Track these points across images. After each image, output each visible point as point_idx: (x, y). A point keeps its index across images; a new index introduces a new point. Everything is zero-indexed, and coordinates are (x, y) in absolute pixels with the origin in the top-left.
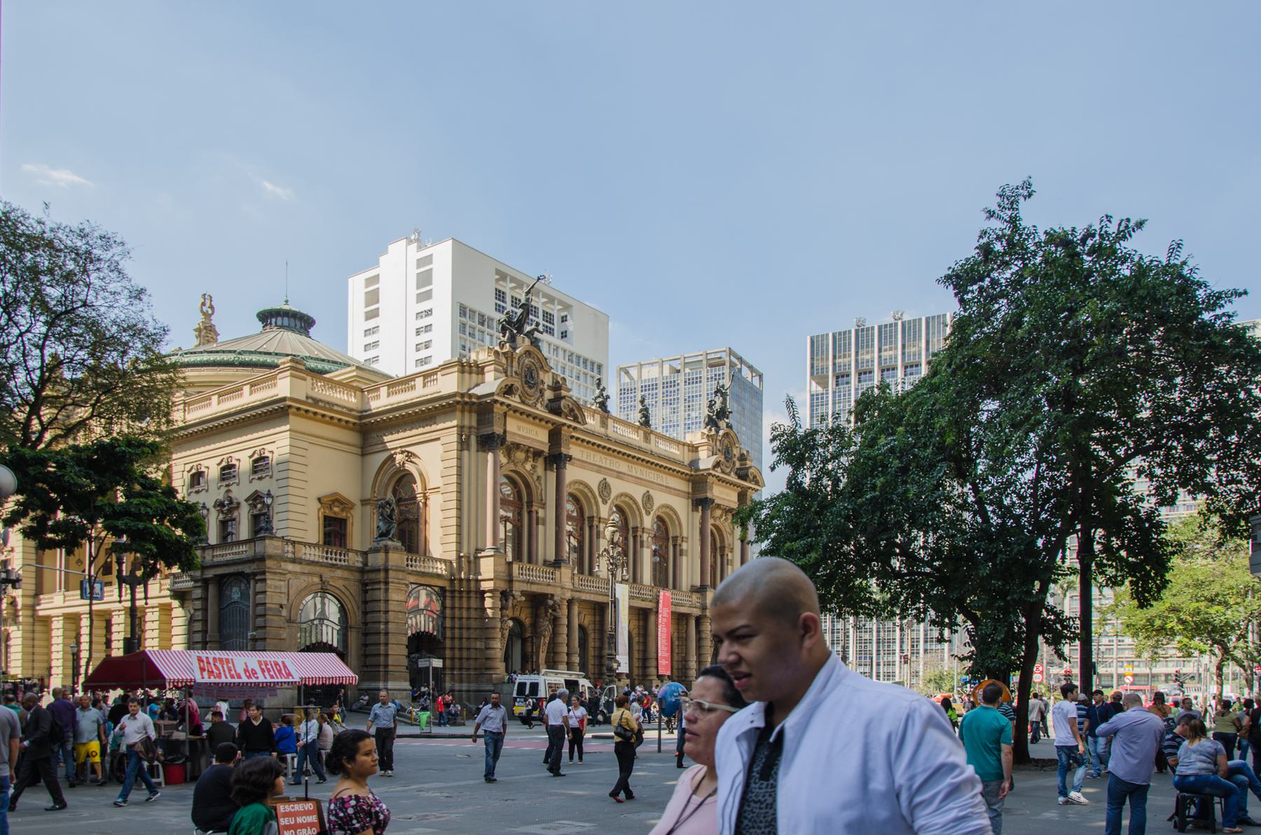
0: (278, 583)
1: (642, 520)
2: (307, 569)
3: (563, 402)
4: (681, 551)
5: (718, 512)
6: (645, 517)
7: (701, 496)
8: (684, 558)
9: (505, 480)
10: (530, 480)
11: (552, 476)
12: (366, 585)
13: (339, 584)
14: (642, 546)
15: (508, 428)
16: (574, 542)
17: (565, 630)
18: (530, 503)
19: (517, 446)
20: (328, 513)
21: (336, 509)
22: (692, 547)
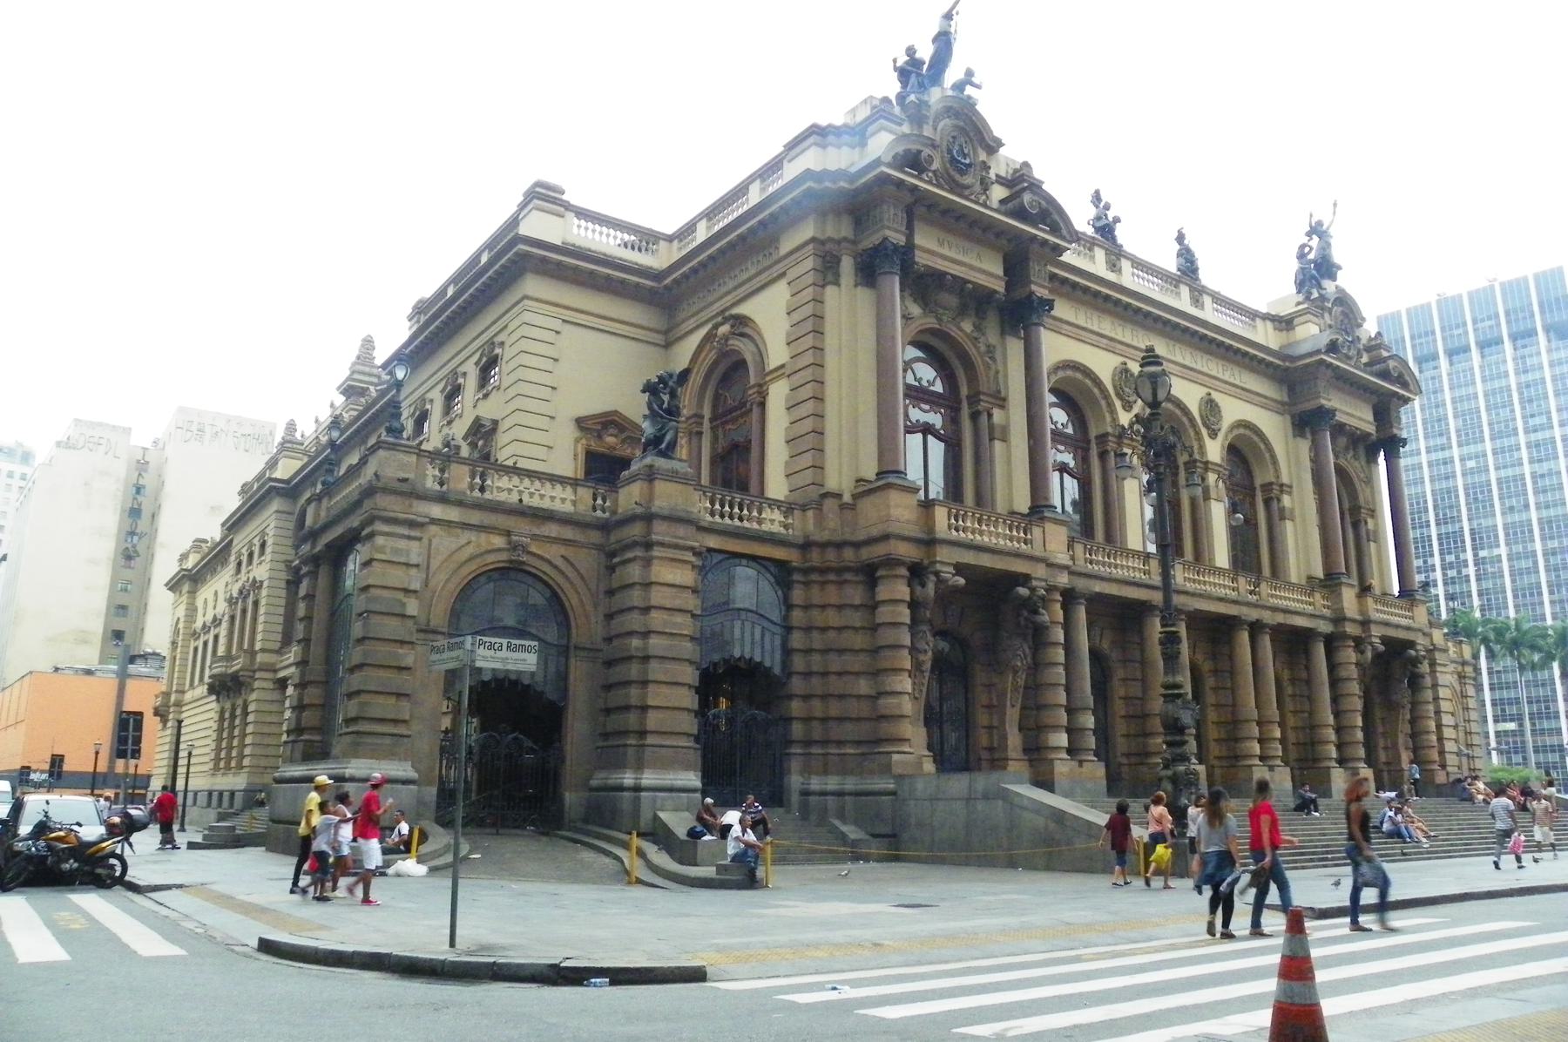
0: (402, 544)
1: (1202, 447)
2: (475, 517)
3: (1027, 198)
4: (1282, 510)
5: (1343, 441)
6: (1208, 442)
7: (1310, 405)
8: (1288, 524)
9: (920, 354)
10: (972, 351)
11: (1014, 349)
12: (612, 555)
13: (553, 552)
14: (1207, 498)
15: (919, 240)
16: (1072, 485)
17: (1060, 655)
18: (974, 399)
19: (939, 276)
20: (595, 446)
21: (610, 440)
22: (1301, 502)
